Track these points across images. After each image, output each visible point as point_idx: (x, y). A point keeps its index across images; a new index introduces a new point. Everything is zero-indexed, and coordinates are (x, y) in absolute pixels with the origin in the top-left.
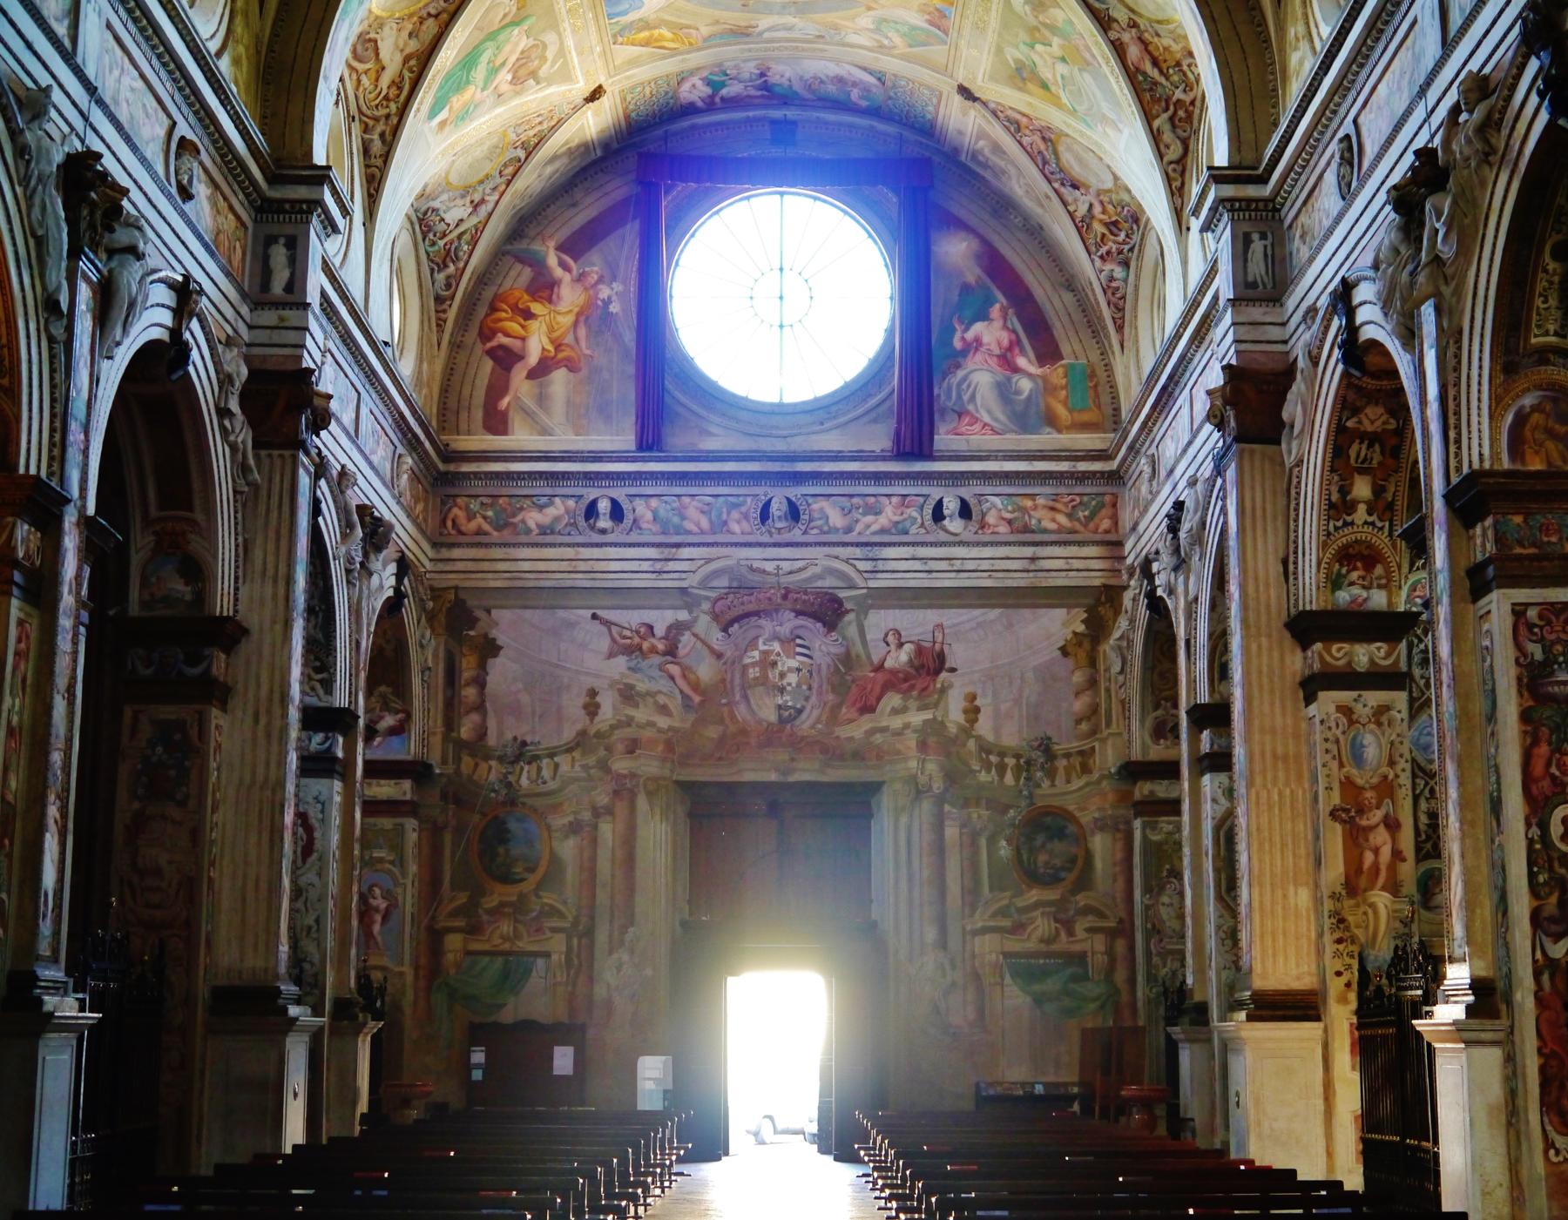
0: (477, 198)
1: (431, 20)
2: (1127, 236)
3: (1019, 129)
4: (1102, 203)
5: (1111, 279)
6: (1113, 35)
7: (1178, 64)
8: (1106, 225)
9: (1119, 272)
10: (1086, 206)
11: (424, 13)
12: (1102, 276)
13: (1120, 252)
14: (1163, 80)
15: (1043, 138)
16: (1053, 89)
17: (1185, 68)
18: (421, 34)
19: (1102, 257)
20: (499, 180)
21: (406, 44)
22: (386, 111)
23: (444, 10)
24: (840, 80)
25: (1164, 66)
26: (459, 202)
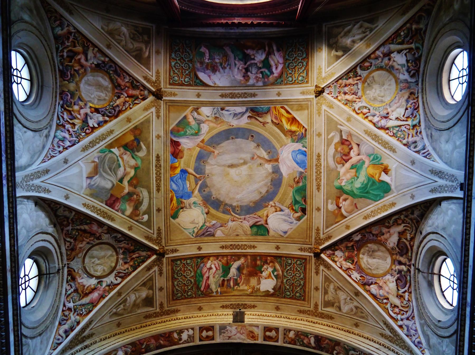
0: (386, 60)
1: (374, 232)
2: (62, 56)
3: (132, 83)
4: (82, 66)
5: (61, 25)
6: (105, 228)
7: (75, 240)
8: (77, 53)
9: (59, 31)
10: (89, 58)
11: (375, 238)
12: (66, 23)
13: (63, 43)
14: (78, 227)
15: (119, 85)
16: (122, 149)
17: (72, 241)
18: (379, 231)
19: (70, 33)
20: (373, 62)
21: (387, 233)
22: (407, 219)
23: (367, 232)
24: (214, 69)
25: (81, 233)
26: (397, 67)
